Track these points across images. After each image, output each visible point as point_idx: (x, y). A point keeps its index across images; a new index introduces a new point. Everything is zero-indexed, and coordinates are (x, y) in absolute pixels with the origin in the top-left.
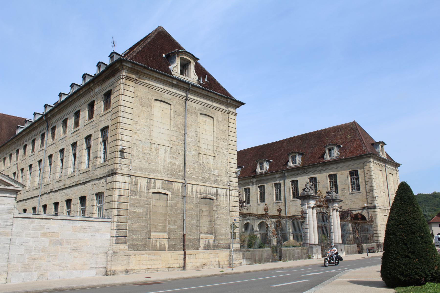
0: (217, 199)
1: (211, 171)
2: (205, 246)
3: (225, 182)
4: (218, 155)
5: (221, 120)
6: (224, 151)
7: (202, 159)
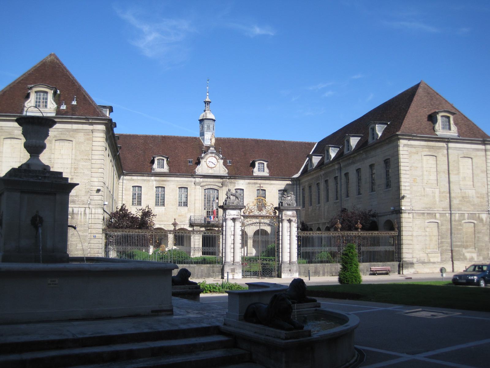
0: (72, 217)
3: (84, 202)
4: (77, 176)
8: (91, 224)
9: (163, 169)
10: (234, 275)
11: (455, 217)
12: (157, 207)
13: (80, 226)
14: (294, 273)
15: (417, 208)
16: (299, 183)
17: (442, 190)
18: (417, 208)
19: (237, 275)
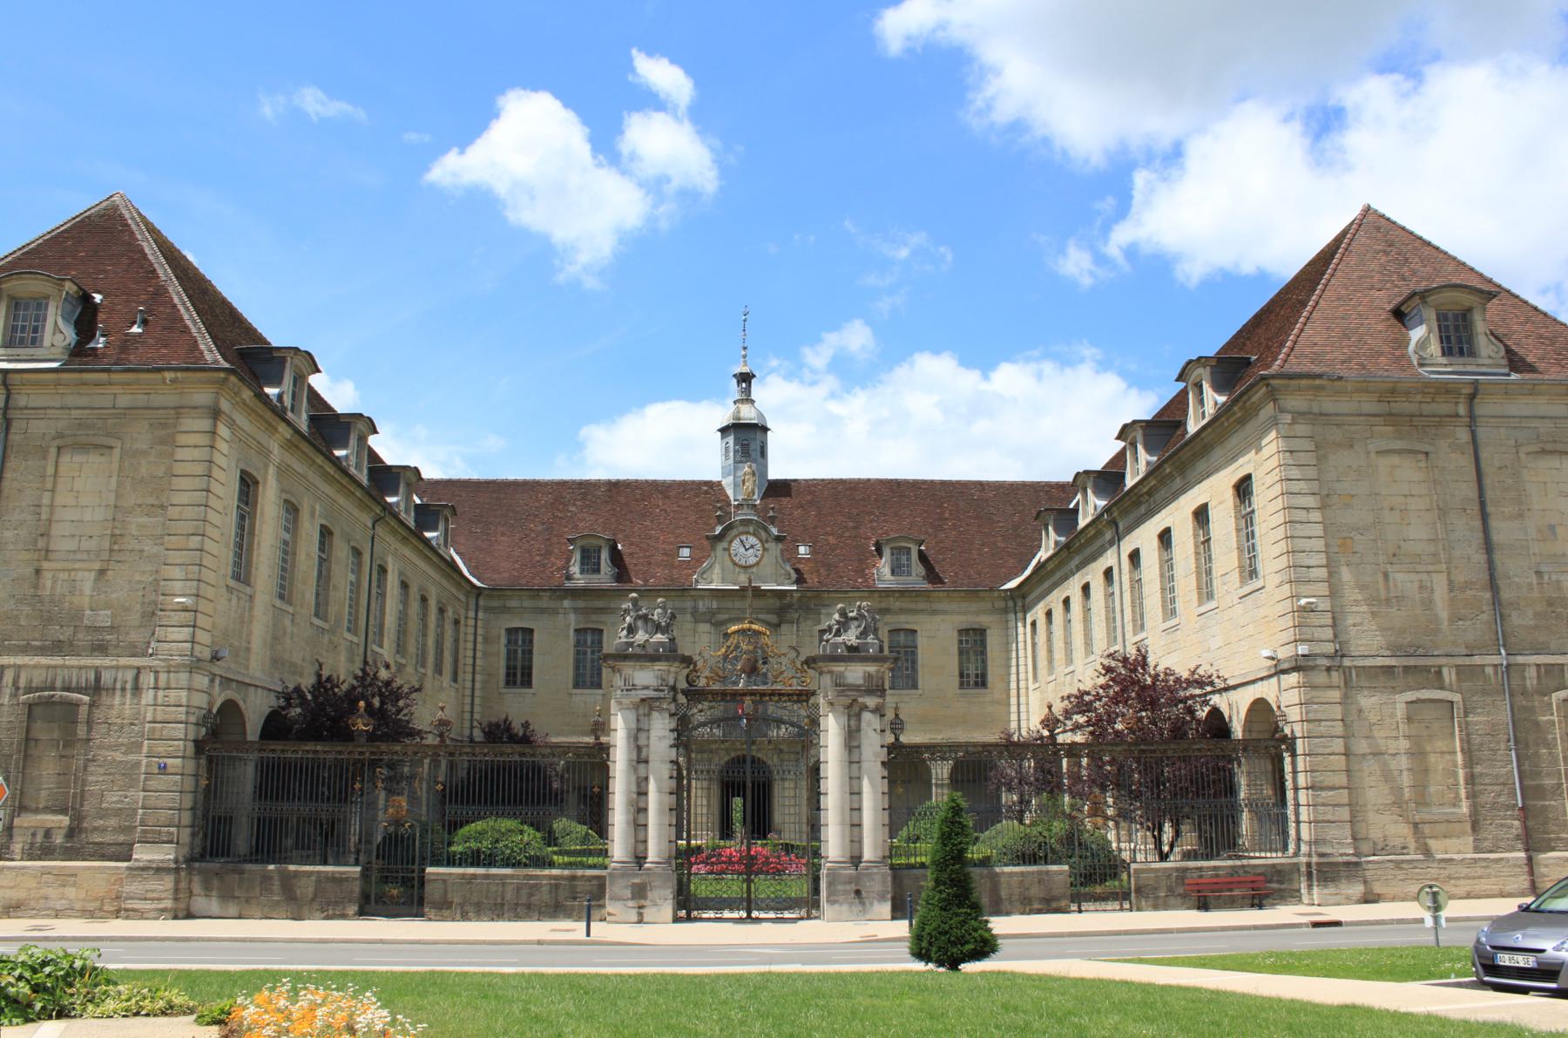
1: (81, 619)
2: (30, 849)
3: (135, 647)
5: (145, 447)
6: (149, 547)
7: (49, 584)
8: (152, 725)
9: (599, 576)
10: (642, 911)
11: (1524, 678)
12: (578, 691)
13: (116, 731)
14: (876, 903)
15: (1361, 648)
16: (1023, 606)
17: (1460, 578)
18: (1361, 648)
19: (654, 909)
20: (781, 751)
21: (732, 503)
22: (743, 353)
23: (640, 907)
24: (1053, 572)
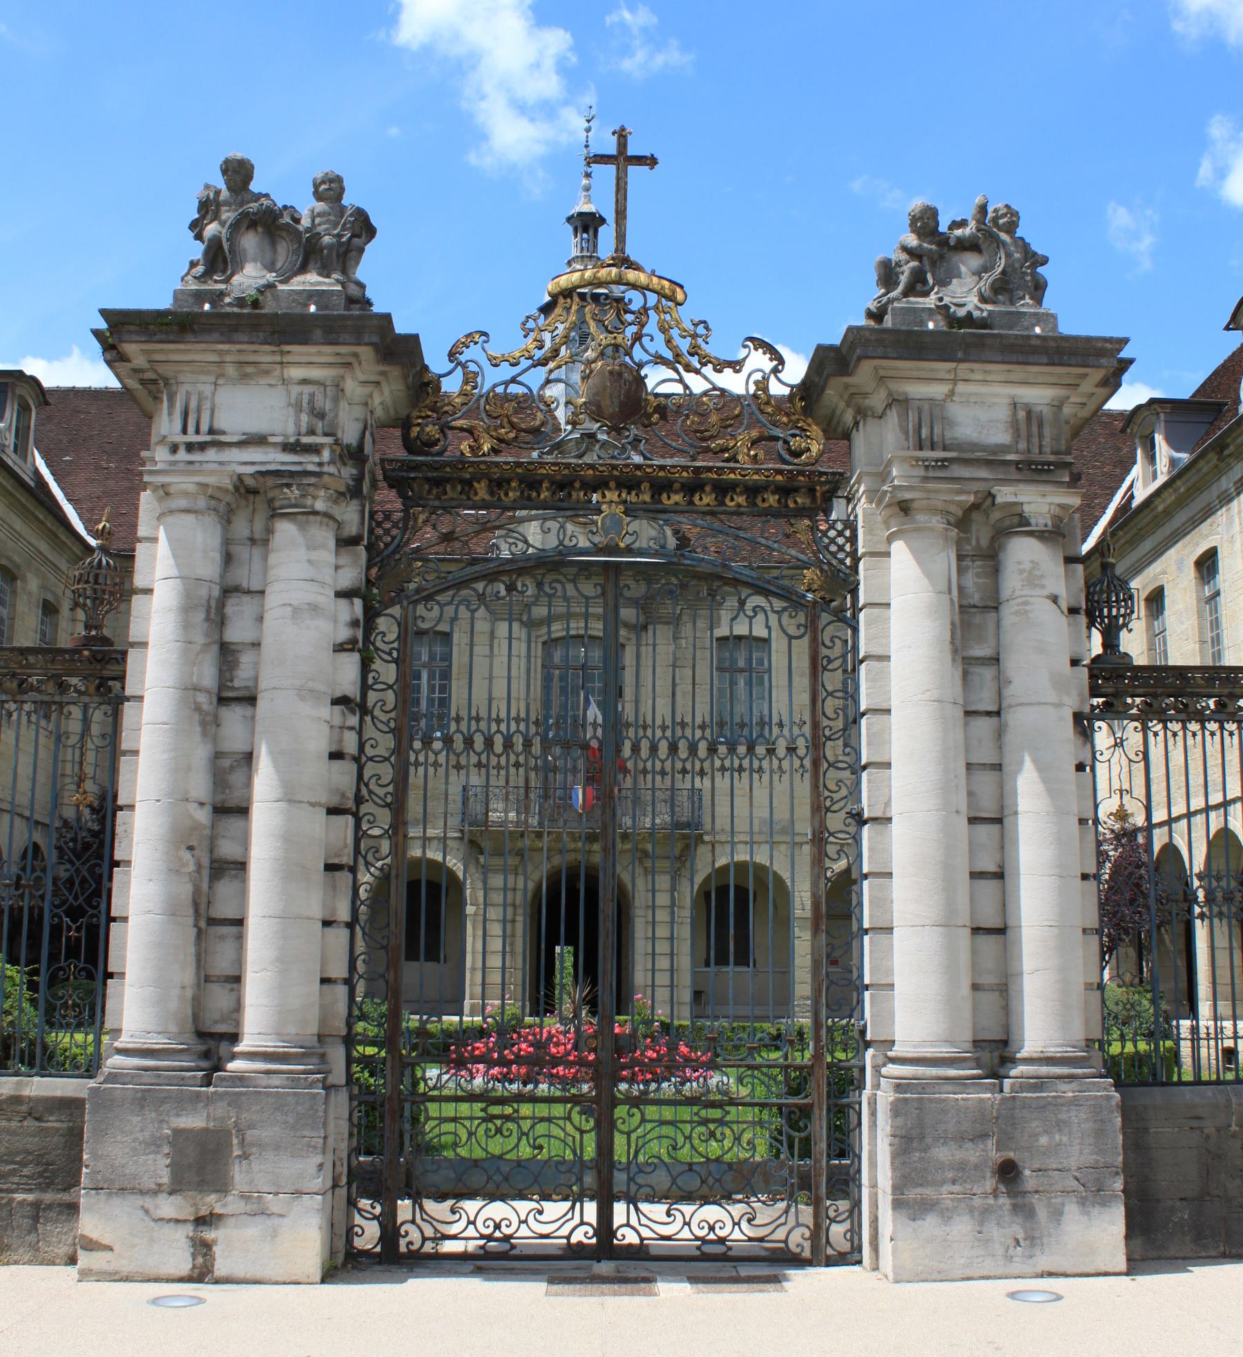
10: (209, 1234)
14: (1072, 1209)
20: (645, 854)
21: (563, 427)
22: (585, 182)
23: (202, 1221)
24: (1168, 514)
